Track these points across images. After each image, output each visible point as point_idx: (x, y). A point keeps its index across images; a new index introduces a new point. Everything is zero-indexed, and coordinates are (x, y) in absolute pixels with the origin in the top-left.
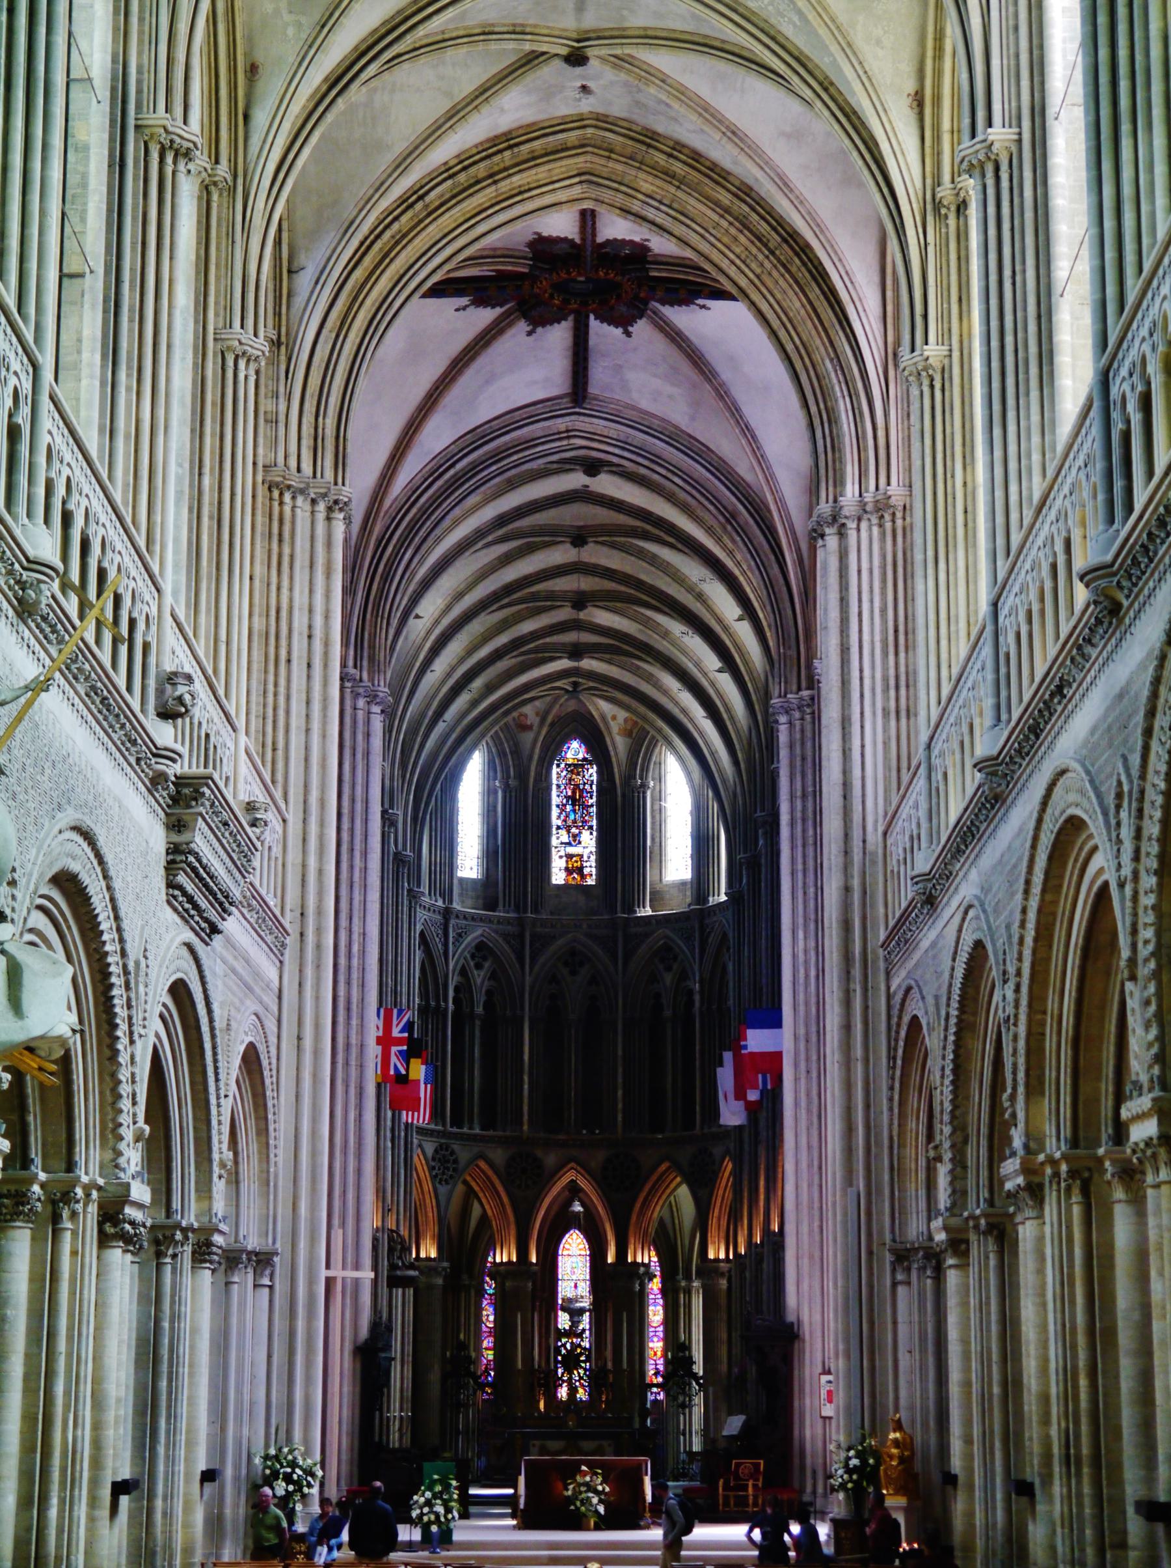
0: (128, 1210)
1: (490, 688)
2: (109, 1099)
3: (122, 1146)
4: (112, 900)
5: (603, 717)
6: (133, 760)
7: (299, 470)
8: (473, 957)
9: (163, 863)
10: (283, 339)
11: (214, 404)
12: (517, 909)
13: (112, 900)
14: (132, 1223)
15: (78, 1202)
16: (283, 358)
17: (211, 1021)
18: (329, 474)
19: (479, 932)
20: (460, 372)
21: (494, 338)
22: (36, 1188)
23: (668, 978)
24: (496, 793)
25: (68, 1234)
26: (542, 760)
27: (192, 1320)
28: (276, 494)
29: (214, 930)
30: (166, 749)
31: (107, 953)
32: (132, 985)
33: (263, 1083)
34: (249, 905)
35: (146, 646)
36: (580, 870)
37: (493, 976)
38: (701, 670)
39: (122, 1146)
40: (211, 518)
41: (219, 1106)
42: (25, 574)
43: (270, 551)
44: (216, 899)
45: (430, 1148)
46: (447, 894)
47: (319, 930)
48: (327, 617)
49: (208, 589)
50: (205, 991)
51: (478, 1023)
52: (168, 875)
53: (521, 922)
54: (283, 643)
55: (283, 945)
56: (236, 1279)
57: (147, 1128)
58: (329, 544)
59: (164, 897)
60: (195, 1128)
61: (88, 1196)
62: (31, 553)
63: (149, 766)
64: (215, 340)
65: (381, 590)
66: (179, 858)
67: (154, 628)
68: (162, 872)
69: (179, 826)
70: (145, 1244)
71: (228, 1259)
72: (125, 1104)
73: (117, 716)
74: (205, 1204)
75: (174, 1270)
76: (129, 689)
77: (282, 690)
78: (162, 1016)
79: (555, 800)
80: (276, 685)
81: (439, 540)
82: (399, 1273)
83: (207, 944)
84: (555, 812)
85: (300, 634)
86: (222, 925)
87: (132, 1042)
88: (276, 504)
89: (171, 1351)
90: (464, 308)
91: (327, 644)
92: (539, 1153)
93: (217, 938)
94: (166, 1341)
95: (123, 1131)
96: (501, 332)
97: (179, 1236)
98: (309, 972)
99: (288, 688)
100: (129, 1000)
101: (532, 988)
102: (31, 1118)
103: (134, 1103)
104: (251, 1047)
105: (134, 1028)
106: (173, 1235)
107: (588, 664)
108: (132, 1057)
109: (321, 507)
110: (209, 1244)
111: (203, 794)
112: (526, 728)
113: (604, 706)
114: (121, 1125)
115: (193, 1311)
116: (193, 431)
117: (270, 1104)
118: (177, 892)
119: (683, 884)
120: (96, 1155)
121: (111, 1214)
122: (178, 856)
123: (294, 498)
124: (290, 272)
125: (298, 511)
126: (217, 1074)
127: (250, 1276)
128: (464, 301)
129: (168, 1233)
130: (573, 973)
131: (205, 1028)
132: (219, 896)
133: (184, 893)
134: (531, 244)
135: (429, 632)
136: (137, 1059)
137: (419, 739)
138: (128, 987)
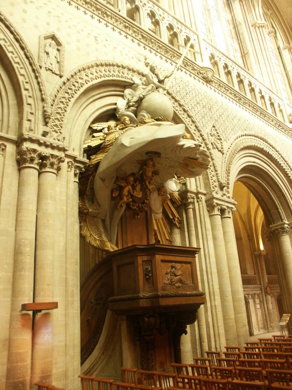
4: (282, 157)
13: (282, 157)
31: (285, 169)
35: (281, 111)
102: (280, 210)
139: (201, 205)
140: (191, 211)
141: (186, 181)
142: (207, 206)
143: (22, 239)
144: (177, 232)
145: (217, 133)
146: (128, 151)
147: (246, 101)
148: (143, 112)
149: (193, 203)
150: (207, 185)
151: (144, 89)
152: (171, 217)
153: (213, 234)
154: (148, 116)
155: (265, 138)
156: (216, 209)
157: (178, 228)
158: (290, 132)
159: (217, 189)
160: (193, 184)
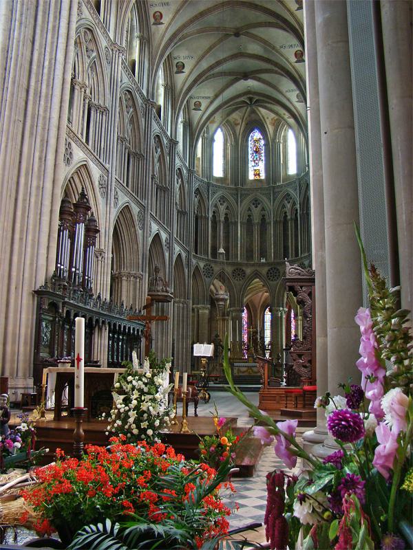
5: (263, 118)
8: (219, 201)
12: (235, 186)
19: (221, 192)
23: (289, 206)
26: (243, 137)
36: (259, 175)
37: (227, 208)
38: (289, 62)
45: (202, 265)
51: (222, 224)
53: (237, 189)
79: (250, 152)
84: (250, 156)
92: (244, 268)
101: (241, 212)
107: (251, 83)
112: (237, 124)
113: (263, 111)
119: (293, 176)
130: (256, 207)
135: (167, 29)
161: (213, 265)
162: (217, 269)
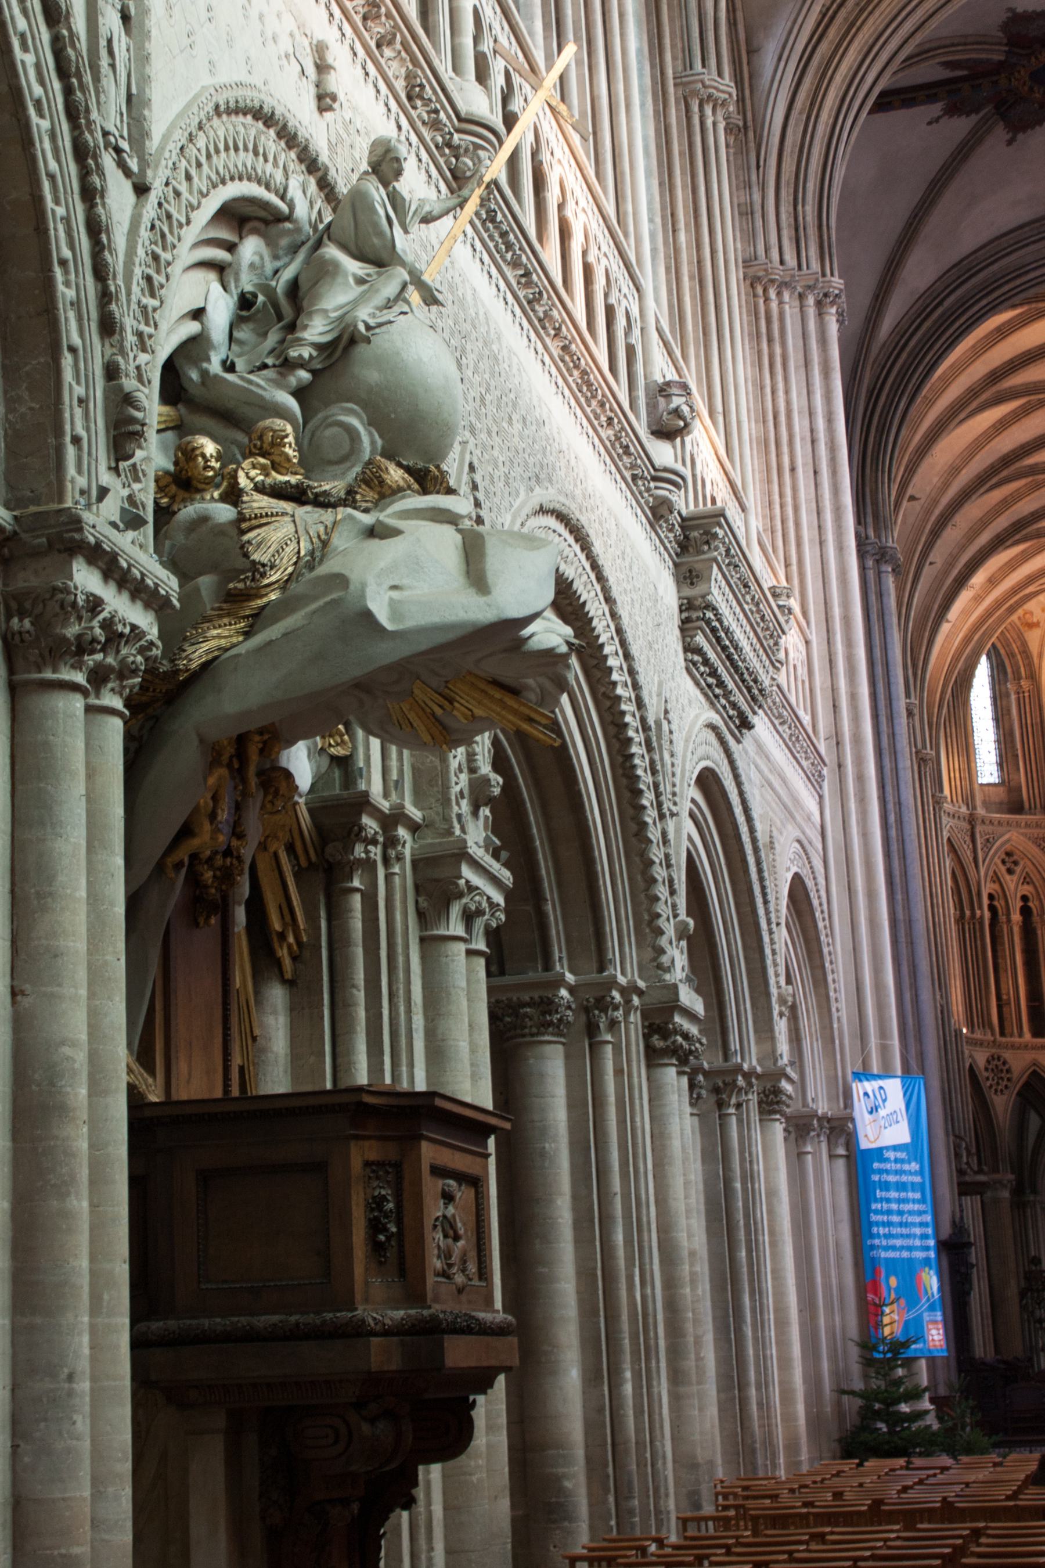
0: (677, 1019)
1: (993, 582)
2: (641, 884)
3: (663, 942)
4: (619, 631)
6: (628, 475)
7: (782, 262)
8: (1003, 862)
9: (676, 622)
10: (750, 123)
11: (681, 154)
14: (686, 1036)
15: (616, 1008)
16: (752, 145)
17: (752, 830)
18: (815, 266)
20: (939, 194)
21: (972, 149)
22: (564, 993)
24: (1008, 695)
25: (609, 1048)
27: (766, 1178)
28: (760, 290)
29: (745, 724)
30: (666, 470)
31: (619, 698)
32: (655, 744)
33: (816, 926)
34: (780, 716)
35: (630, 350)
39: (663, 942)
40: (691, 278)
41: (771, 932)
42: (456, 136)
43: (760, 352)
44: (743, 681)
45: (981, 1058)
46: (969, 799)
47: (859, 761)
48: (830, 420)
49: (697, 356)
50: (741, 793)
52: (684, 637)
54: (785, 449)
55: (820, 775)
56: (809, 1149)
57: (691, 922)
58: (823, 341)
59: (683, 664)
60: (746, 958)
61: (628, 1001)
62: (463, 108)
63: (648, 490)
64: (675, 85)
65: (878, 444)
66: (694, 615)
67: (636, 332)
68: (677, 632)
69: (691, 577)
70: (704, 1092)
71: (797, 1126)
72: (662, 891)
73: (602, 405)
74: (767, 1046)
75: (740, 1121)
76: (613, 368)
77: (789, 499)
78: (692, 815)
80: (781, 495)
81: (931, 403)
82: (967, 1179)
83: (739, 742)
85: (802, 439)
86: (755, 720)
87: (662, 816)
88: (761, 301)
89: (747, 1216)
90: (937, 120)
91: (832, 448)
93: (748, 736)
94: (740, 1204)
95: (662, 922)
96: (980, 141)
97: (741, 1081)
98: (852, 805)
99: (795, 497)
100: (652, 762)
103: (673, 892)
104: (797, 879)
105: (663, 798)
106: (735, 1081)
108: (664, 834)
109: (811, 300)
110: (777, 1091)
111: (716, 535)
112: (1031, 626)
114: (659, 916)
115: (766, 1170)
116: (661, 184)
117: (825, 950)
118: (696, 658)
120: (632, 953)
121: (659, 1021)
122: (694, 614)
123: (779, 294)
124: (748, 52)
125: (787, 307)
126: (764, 895)
127: (824, 1146)
128: (936, 109)
129: (728, 1079)
131: (746, 838)
132: (746, 676)
133: (706, 662)
134: (1005, 27)
135: (929, 512)
136: (671, 836)
137: (927, 634)
138: (650, 748)
139: (397, 880)
140: (356, 901)
141: (355, 748)
142: (417, 888)
143: (63, 1043)
144: (277, 995)
145: (477, 504)
146: (386, 654)
147: (555, 313)
148: (351, 412)
149: (369, 865)
150: (431, 785)
151: (360, 281)
152: (277, 926)
153: (430, 1034)
154: (373, 443)
155: (584, 519)
156: (455, 910)
157: (284, 981)
158: (648, 490)
159: (465, 806)
160: (381, 768)
161: (1007, 1055)
162: (1019, 1063)
